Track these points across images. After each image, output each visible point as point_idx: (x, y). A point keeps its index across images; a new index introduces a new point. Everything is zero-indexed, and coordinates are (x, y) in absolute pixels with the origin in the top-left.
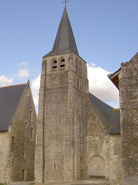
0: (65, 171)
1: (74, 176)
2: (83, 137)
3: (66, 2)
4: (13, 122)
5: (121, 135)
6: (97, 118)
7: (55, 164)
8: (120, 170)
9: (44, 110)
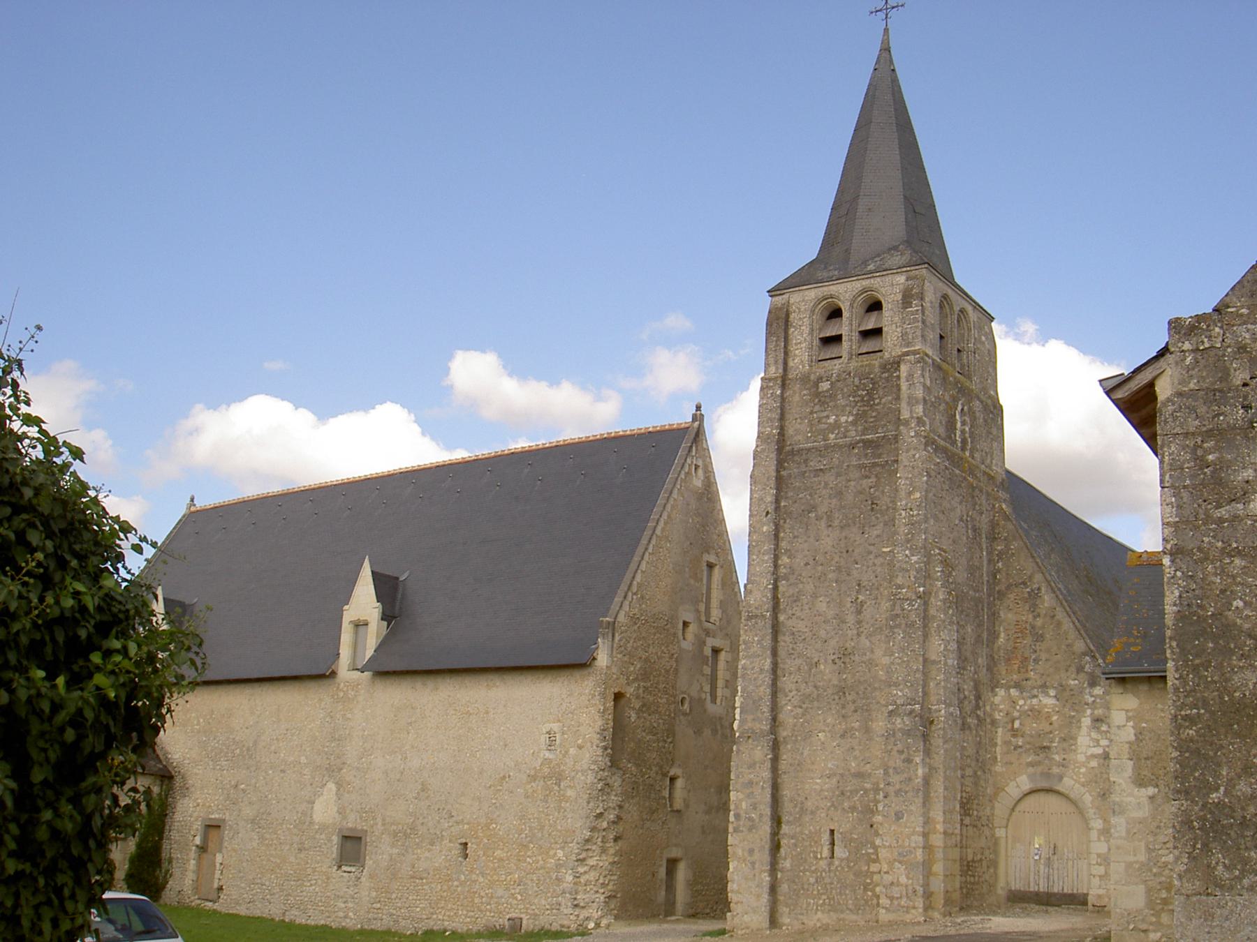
0: (885, 868)
1: (928, 895)
2: (978, 697)
3: (886, 9)
4: (621, 618)
5: (1170, 683)
6: (1047, 600)
7: (832, 832)
8: (1166, 864)
9: (776, 558)
